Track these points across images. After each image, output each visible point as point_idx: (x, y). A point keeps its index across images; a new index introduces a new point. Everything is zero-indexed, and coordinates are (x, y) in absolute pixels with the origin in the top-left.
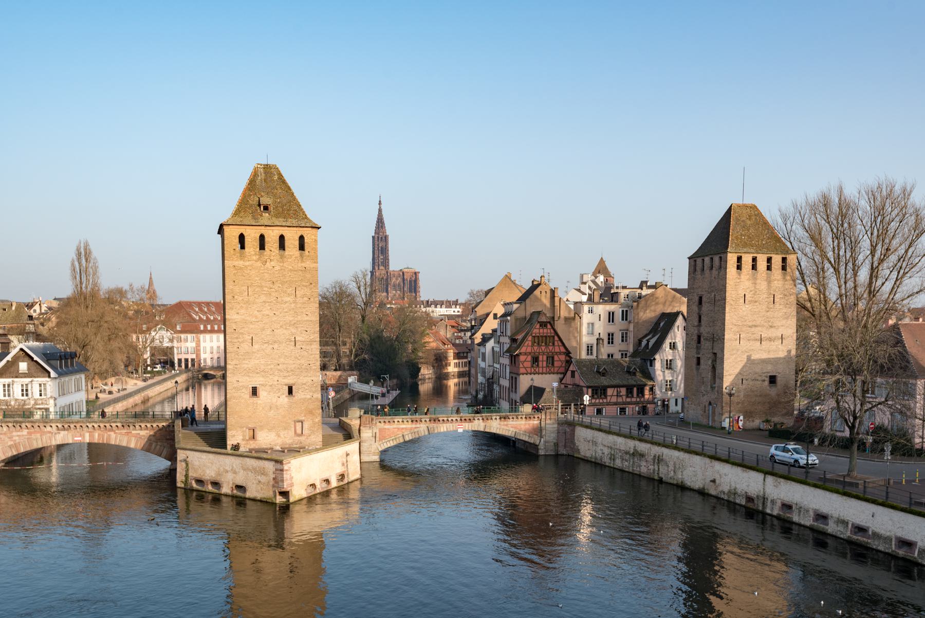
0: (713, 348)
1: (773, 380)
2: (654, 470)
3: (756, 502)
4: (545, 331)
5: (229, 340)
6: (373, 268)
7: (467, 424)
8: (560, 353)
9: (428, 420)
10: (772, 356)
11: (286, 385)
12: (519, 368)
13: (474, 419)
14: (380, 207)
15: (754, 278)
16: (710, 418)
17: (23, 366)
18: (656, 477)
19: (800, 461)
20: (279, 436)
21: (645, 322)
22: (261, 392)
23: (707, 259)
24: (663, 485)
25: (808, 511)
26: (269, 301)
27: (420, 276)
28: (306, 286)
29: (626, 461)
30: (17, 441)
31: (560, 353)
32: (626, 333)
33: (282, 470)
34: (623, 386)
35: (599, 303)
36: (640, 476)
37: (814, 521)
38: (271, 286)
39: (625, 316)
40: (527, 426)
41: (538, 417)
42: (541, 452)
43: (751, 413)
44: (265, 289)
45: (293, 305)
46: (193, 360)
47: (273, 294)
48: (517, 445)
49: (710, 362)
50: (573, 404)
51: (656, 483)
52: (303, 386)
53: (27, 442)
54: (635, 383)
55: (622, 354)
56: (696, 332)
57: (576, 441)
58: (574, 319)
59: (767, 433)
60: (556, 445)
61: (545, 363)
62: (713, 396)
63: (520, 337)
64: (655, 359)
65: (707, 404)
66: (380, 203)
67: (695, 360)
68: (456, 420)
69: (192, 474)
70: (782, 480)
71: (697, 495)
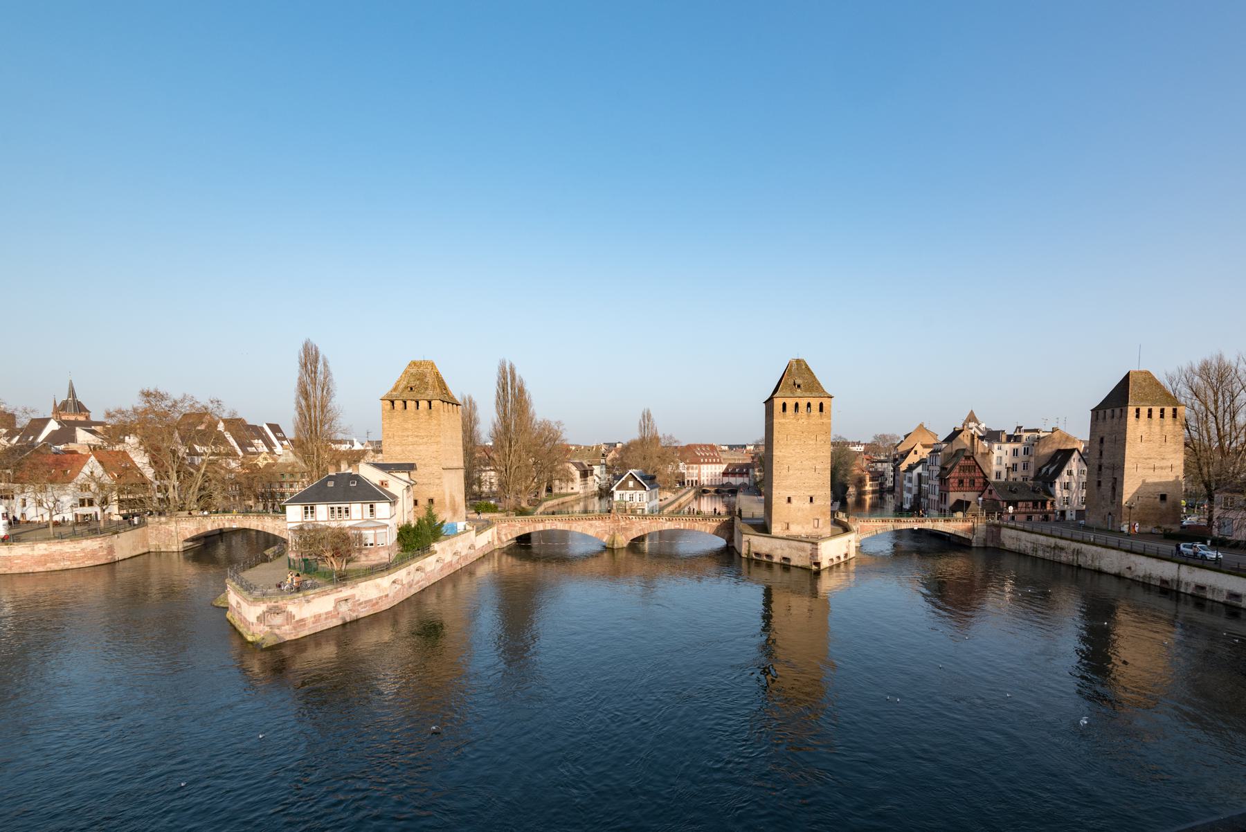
1: (1163, 497)
3: (1170, 584)
4: (969, 462)
8: (980, 477)
10: (1163, 480)
12: (948, 487)
19: (1207, 555)
21: (1044, 455)
25: (1221, 591)
31: (980, 477)
34: (1030, 501)
35: (1004, 443)
37: (1227, 598)
39: (1026, 451)
43: (1145, 521)
49: (1110, 484)
50: (996, 513)
54: (1039, 499)
55: (1024, 479)
56: (1098, 462)
58: (988, 454)
59: (1162, 536)
61: (968, 484)
62: (1112, 509)
63: (949, 466)
64: (1055, 482)
65: (1107, 514)
67: (1096, 483)
70: (1196, 569)
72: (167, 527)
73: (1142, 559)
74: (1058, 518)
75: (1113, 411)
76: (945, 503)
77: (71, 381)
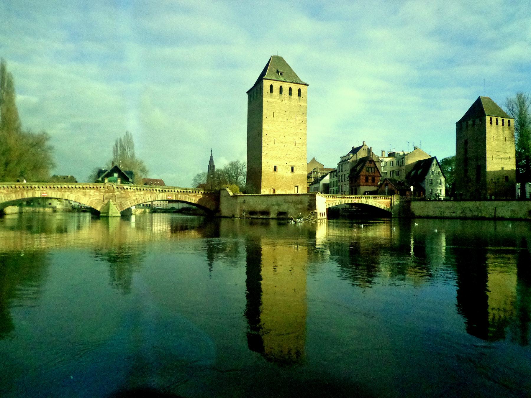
5: (264, 140)
7: (358, 200)
9: (340, 197)
11: (290, 166)
12: (360, 182)
13: (361, 198)
14: (212, 153)
26: (284, 121)
28: (301, 115)
29: (454, 213)
30: (138, 197)
32: (399, 172)
33: (315, 200)
38: (285, 113)
39: (398, 163)
40: (385, 202)
41: (390, 198)
44: (282, 114)
45: (295, 124)
46: (150, 205)
47: (285, 117)
52: (299, 167)
53: (143, 198)
66: (212, 152)
68: (353, 197)
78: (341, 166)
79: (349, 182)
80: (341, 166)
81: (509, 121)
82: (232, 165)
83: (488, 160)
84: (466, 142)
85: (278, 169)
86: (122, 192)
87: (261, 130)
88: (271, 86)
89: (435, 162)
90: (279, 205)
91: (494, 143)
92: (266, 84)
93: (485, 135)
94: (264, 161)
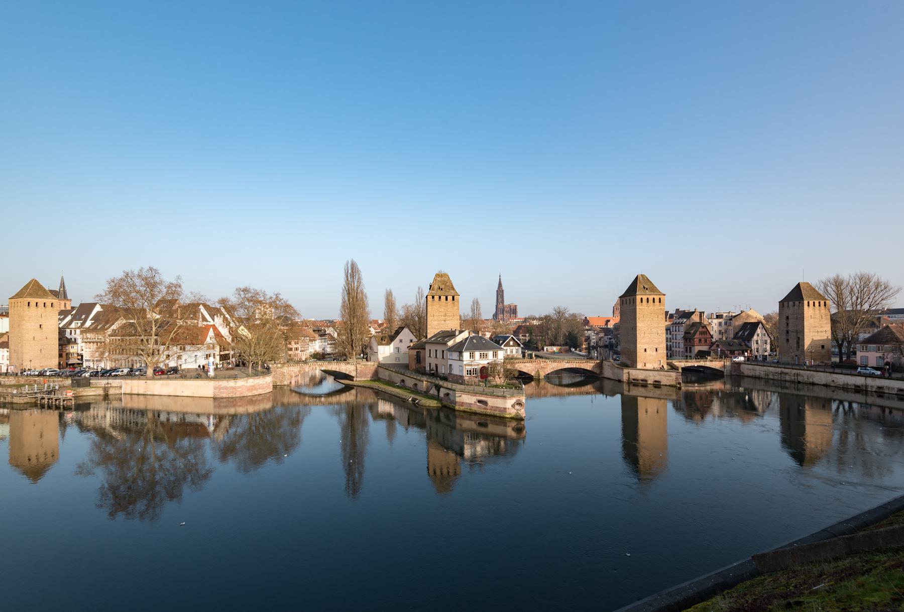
0: (797, 335)
1: (823, 347)
2: (795, 379)
3: (861, 387)
6: (497, 304)
10: (822, 338)
15: (814, 309)
16: (797, 361)
17: (511, 343)
18: (796, 381)
20: (653, 365)
21: (738, 326)
22: (647, 350)
23: (791, 303)
24: (801, 384)
27: (518, 307)
36: (786, 381)
39: (726, 323)
42: (725, 374)
48: (705, 371)
49: (795, 340)
51: (796, 384)
57: (741, 369)
60: (730, 371)
62: (798, 353)
65: (794, 356)
67: (785, 340)
69: (631, 377)
71: (822, 386)
72: (282, 370)
73: (841, 376)
74: (754, 359)
75: (794, 303)
76: (690, 352)
77: (62, 277)
78: (674, 327)
79: (683, 341)
80: (674, 327)
81: (825, 303)
82: (559, 313)
83: (805, 334)
84: (788, 318)
85: (647, 350)
86: (545, 364)
87: (636, 326)
88: (642, 299)
89: (760, 325)
90: (655, 376)
91: (811, 321)
92: (638, 298)
93: (804, 314)
94: (638, 346)
